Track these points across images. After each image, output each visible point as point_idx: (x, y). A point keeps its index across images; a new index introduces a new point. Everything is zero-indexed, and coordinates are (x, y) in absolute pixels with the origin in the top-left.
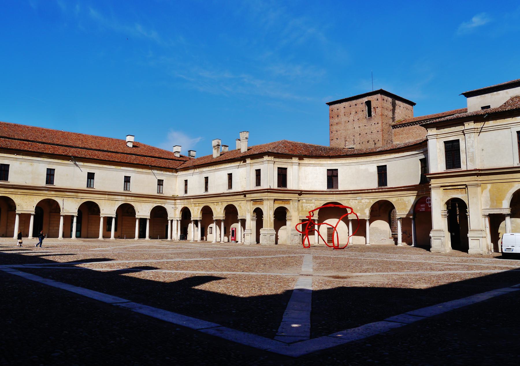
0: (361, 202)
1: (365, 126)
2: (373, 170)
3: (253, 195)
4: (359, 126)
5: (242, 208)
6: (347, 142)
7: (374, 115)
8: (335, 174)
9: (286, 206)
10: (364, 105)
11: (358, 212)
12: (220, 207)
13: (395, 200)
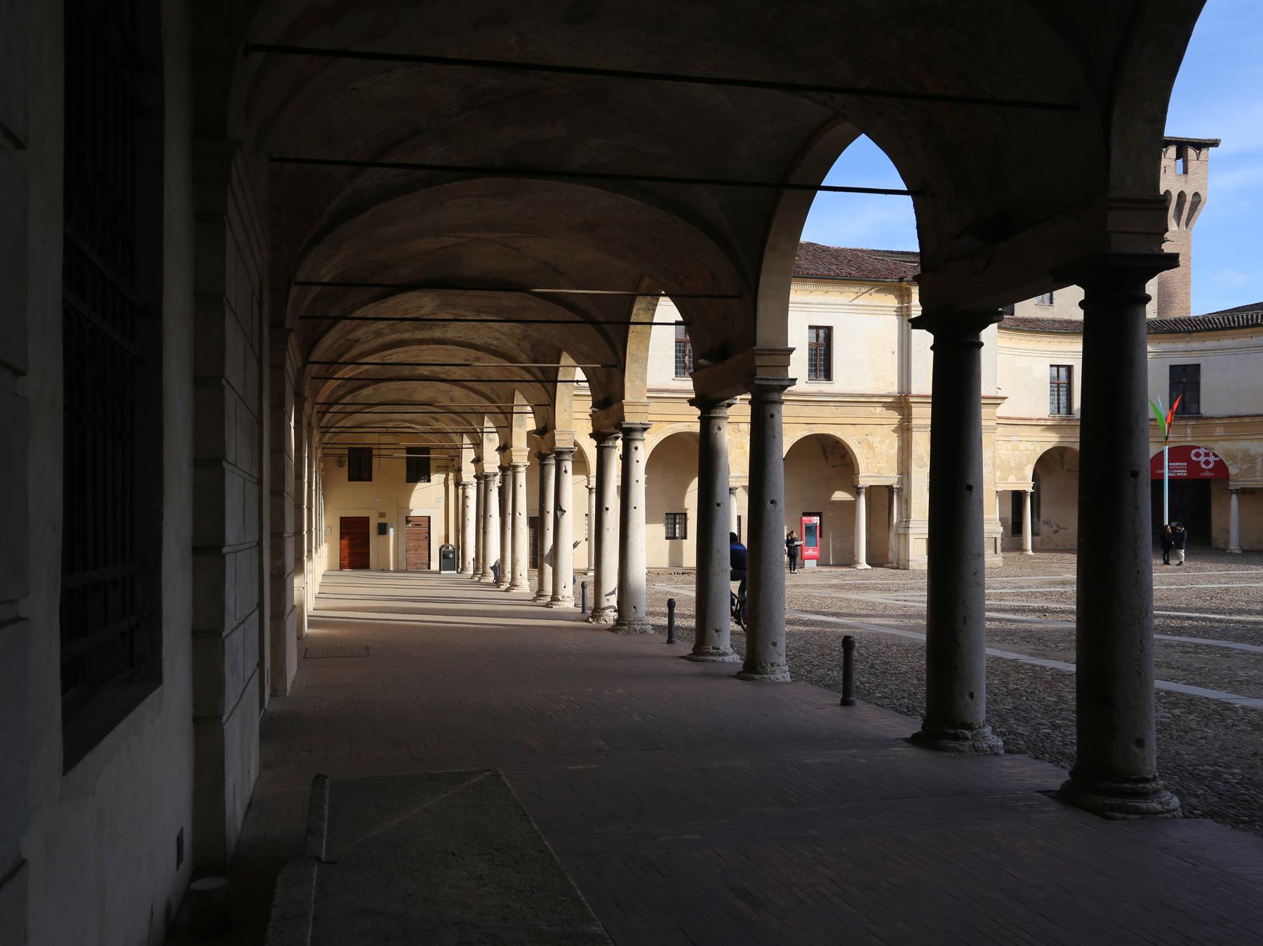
5: (876, 450)
11: (1013, 473)
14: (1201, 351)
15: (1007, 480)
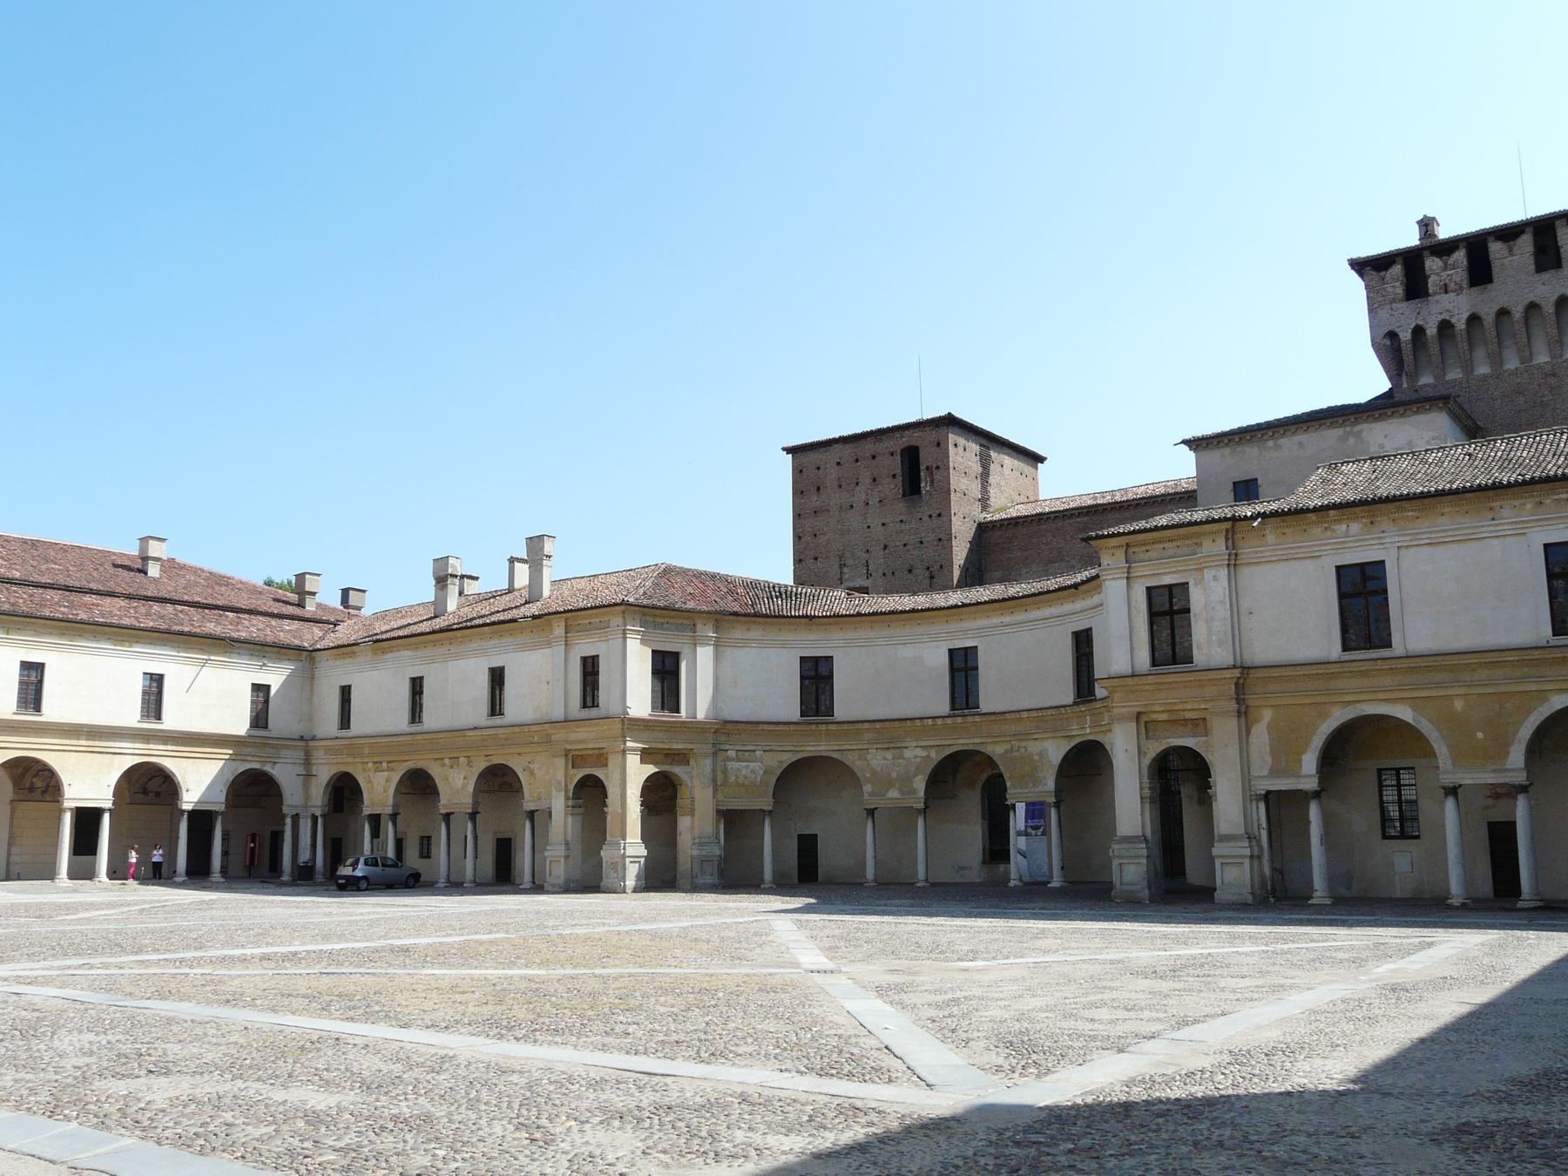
0: (901, 757)
1: (902, 521)
4: (884, 521)
6: (846, 570)
7: (928, 488)
8: (823, 670)
9: (677, 770)
10: (898, 458)
12: (464, 773)
14: (1081, 611)
15: (885, 796)
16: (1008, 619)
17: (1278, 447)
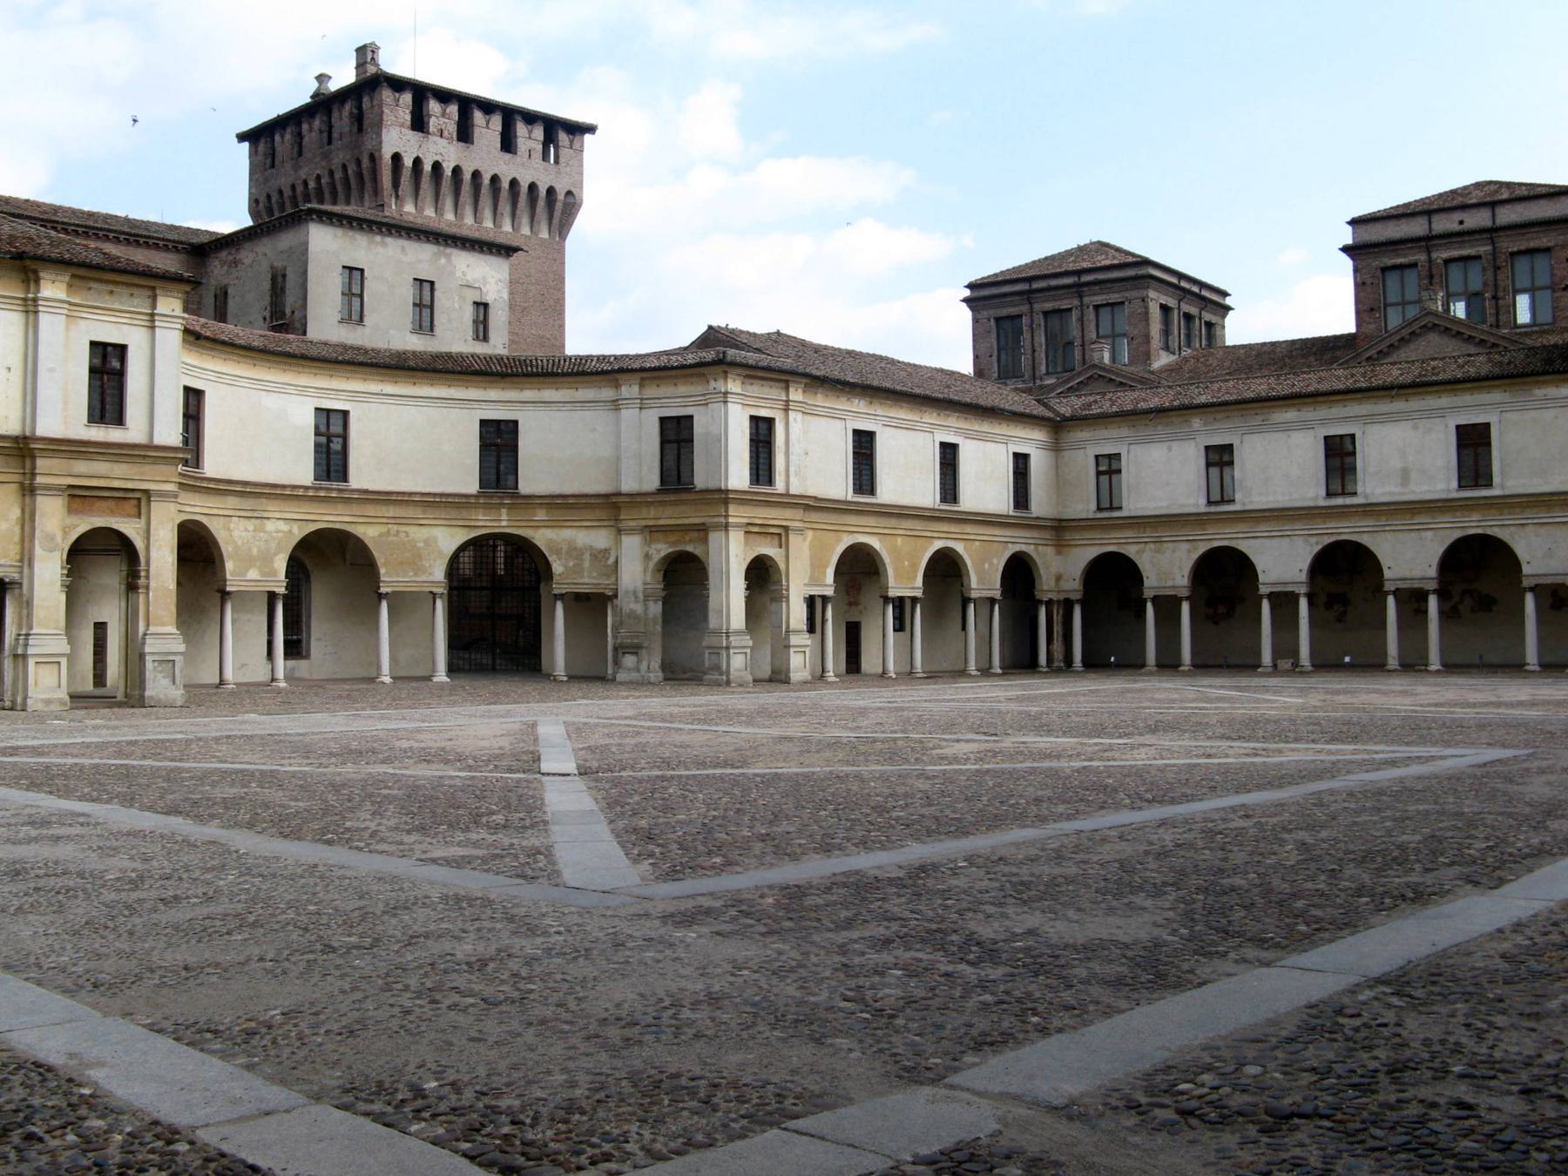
2: (302, 416)
3: (81, 466)
13: (376, 534)
15: (245, 575)
16: (389, 388)
17: (384, 245)
